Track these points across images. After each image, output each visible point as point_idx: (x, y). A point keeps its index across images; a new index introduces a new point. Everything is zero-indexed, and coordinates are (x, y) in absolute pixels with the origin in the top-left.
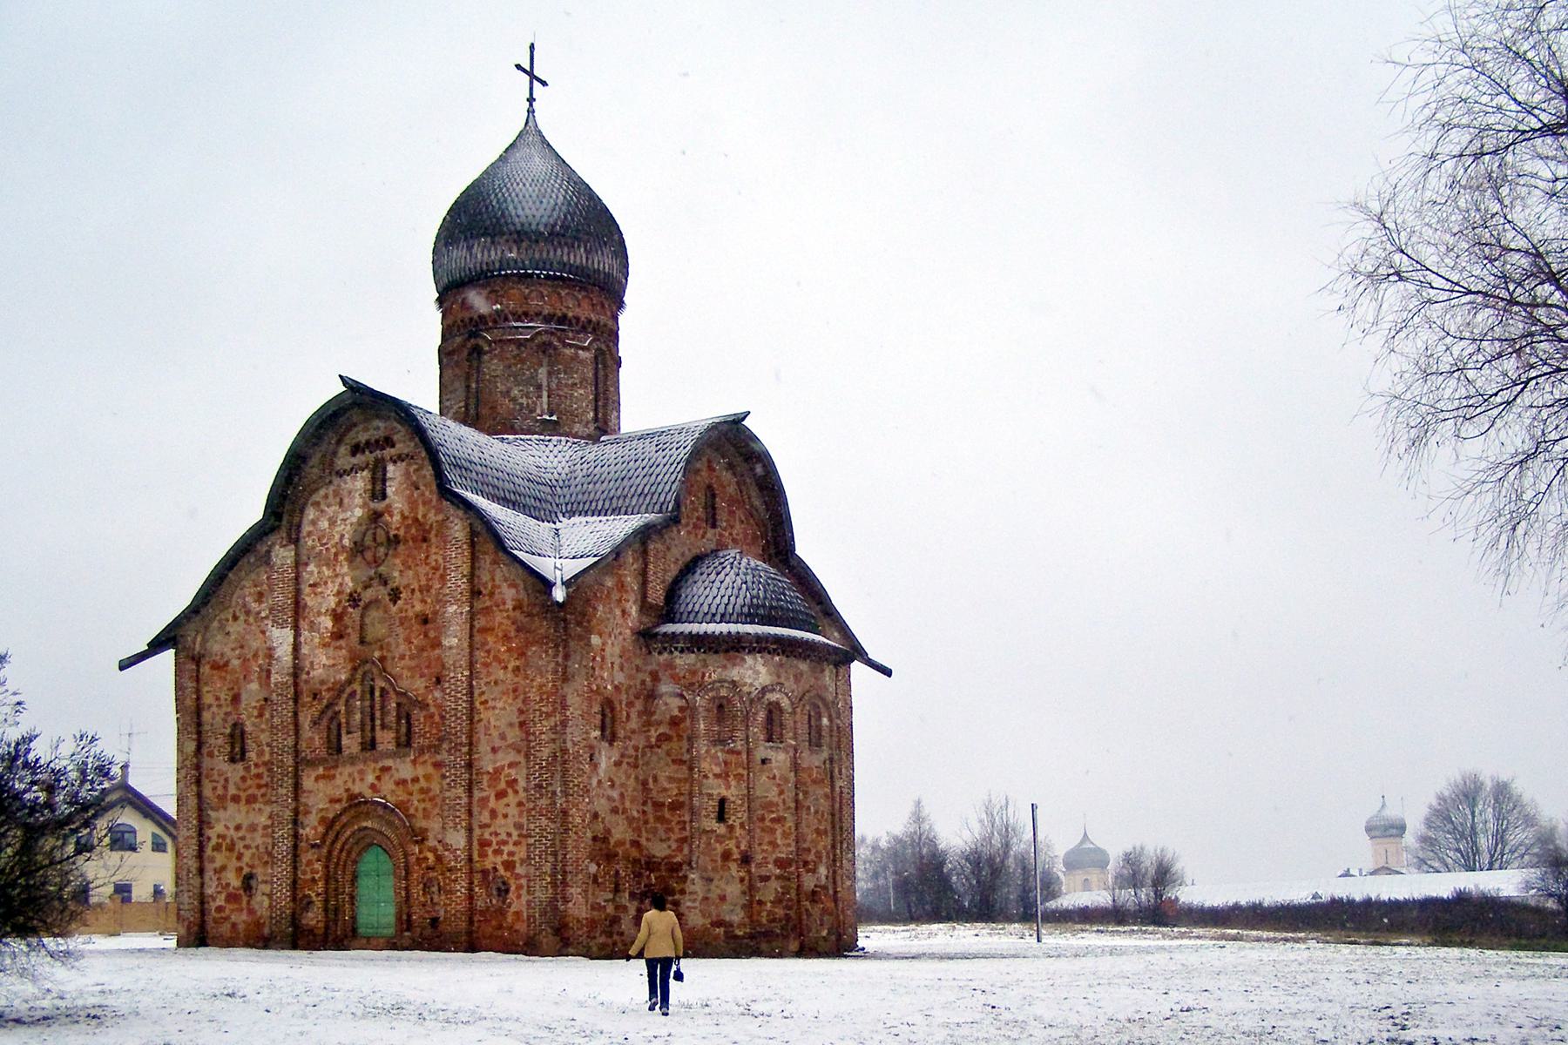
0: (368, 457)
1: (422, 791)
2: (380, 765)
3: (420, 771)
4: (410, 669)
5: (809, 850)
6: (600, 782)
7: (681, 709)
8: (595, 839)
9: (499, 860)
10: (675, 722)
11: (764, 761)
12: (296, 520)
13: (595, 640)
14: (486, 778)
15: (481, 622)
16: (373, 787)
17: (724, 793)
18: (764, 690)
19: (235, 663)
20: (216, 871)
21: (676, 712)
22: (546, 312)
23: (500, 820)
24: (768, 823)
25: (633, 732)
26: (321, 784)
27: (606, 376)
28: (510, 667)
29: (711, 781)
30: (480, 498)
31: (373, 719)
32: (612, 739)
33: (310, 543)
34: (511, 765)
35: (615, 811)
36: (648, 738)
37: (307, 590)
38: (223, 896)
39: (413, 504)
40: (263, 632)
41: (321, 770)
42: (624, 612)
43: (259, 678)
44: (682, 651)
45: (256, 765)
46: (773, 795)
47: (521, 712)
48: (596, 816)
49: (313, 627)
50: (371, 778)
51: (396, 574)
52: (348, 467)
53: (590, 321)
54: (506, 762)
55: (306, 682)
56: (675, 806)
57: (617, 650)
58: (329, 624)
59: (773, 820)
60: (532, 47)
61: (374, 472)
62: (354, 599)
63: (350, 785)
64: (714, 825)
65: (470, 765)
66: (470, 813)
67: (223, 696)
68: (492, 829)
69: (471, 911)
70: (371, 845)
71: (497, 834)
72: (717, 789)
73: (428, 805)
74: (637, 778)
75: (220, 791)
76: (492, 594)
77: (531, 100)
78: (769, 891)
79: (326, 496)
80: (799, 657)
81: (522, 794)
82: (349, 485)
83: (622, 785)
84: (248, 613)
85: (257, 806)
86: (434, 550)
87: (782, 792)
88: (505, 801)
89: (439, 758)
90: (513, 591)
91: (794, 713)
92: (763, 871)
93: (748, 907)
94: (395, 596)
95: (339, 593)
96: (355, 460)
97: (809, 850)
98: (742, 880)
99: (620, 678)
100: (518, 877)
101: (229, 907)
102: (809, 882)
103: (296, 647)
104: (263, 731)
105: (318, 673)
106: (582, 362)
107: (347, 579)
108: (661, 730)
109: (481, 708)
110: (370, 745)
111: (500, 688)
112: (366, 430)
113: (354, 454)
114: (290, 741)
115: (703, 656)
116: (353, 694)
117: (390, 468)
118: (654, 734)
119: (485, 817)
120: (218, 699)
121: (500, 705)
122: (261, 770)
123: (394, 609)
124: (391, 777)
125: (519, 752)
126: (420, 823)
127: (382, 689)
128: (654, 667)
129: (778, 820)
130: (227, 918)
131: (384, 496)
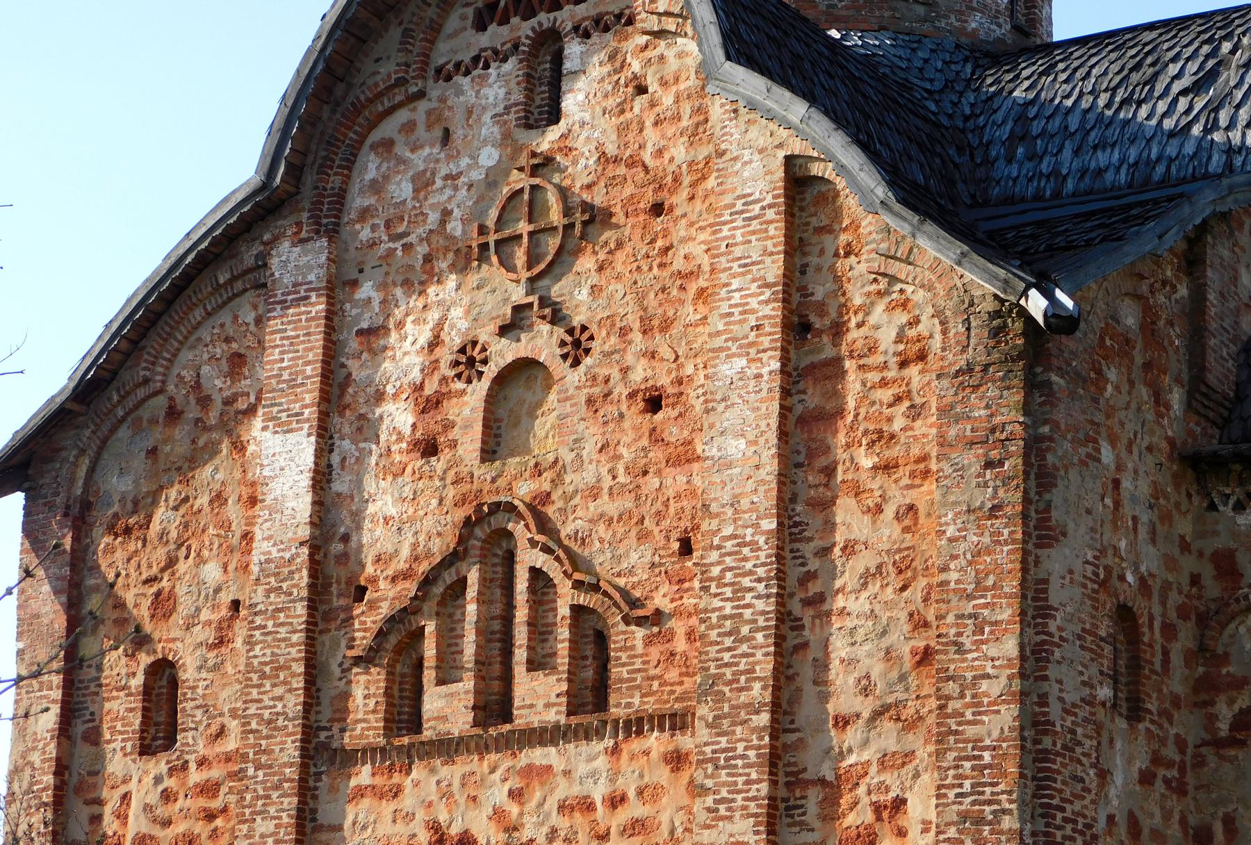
0: (524, 29)
6: (1111, 819)
12: (335, 181)
25: (1176, 702)
28: (889, 511)
31: (507, 653)
32: (1135, 713)
36: (1212, 718)
37: (354, 344)
45: (201, 763)
47: (919, 623)
52: (467, 58)
57: (1144, 488)
61: (531, 59)
62: (469, 360)
74: (1183, 822)
76: (838, 329)
79: (409, 127)
82: (470, 96)
84: (205, 402)
94: (577, 347)
96: (484, 40)
99: (1151, 561)
103: (322, 478)
107: (456, 313)
110: (494, 706)
113: (481, 26)
114: (294, 703)
116: (462, 583)
118: (1225, 713)
122: (216, 773)
123: (573, 377)
128: (1220, 542)
131: (554, 115)
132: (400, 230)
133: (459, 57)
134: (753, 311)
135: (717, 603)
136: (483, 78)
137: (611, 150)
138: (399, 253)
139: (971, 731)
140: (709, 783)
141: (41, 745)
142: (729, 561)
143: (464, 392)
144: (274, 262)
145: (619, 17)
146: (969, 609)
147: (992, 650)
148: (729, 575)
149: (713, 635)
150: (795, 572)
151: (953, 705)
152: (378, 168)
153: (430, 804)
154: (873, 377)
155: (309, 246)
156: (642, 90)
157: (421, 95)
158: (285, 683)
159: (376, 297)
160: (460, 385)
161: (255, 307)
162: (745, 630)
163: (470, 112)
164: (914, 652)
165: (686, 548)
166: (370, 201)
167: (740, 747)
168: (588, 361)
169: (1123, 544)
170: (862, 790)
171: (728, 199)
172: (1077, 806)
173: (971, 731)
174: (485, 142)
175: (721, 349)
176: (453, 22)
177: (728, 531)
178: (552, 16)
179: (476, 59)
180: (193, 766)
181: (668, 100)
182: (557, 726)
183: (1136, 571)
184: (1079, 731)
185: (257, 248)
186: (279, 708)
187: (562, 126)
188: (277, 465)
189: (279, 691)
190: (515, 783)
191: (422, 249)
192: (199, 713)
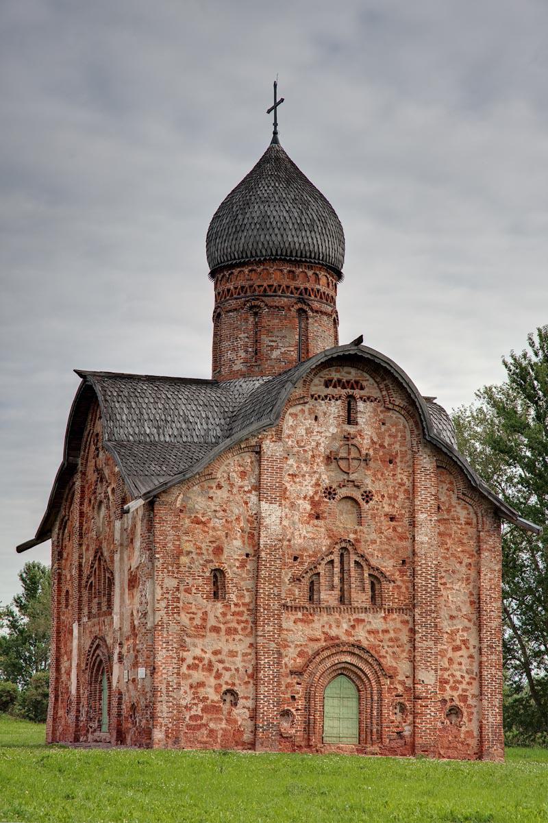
0: (344, 392)
1: (391, 640)
2: (355, 616)
3: (391, 625)
4: (381, 550)
9: (455, 694)
14: (445, 636)
16: (348, 633)
19: (217, 523)
20: (191, 687)
23: (456, 666)
26: (300, 626)
28: (464, 564)
33: (290, 443)
34: (466, 629)
38: (201, 705)
39: (380, 435)
40: (246, 503)
41: (300, 615)
43: (243, 537)
49: (293, 505)
50: (345, 626)
51: (368, 481)
55: (289, 546)
58: (308, 507)
62: (330, 493)
63: (326, 629)
67: (204, 546)
68: (449, 672)
70: (342, 674)
71: (453, 676)
73: (396, 649)
75: (198, 622)
76: (449, 511)
79: (303, 411)
81: (472, 650)
84: (232, 485)
85: (237, 637)
86: (399, 470)
88: (459, 653)
89: (407, 618)
90: (466, 512)
94: (368, 496)
95: (317, 485)
100: (469, 706)
101: (206, 717)
104: (243, 579)
105: (298, 541)
109: (442, 587)
111: (457, 576)
112: (337, 371)
113: (327, 386)
116: (332, 562)
117: (361, 406)
119: (445, 663)
120: (200, 548)
121: (456, 587)
122: (242, 609)
124: (372, 627)
125: (470, 621)
126: (388, 662)
127: (356, 562)
130: (206, 725)
132: (302, 445)
133: (320, 394)
134: (429, 502)
135: (420, 581)
136: (330, 404)
137: (375, 440)
138: (302, 452)
139: (489, 624)
140: (420, 631)
141: (171, 592)
142: (424, 570)
143: (327, 502)
144: (264, 446)
145: (376, 399)
146: (488, 593)
147: (494, 604)
148: (424, 574)
149: (419, 590)
151: (485, 617)
152: (293, 422)
153: (324, 626)
154: (459, 526)
155: (276, 444)
156: (383, 424)
157: (306, 403)
158: (274, 584)
159: (295, 465)
160: (326, 500)
161: (251, 457)
162: (429, 590)
163: (325, 414)
164: (471, 601)
165: (404, 562)
166: (292, 432)
167: (429, 621)
168: (371, 502)
170: (458, 635)
171: (419, 467)
173: (489, 624)
174: (331, 425)
175: (420, 510)
176: (316, 381)
177: (424, 562)
178: (352, 391)
179: (326, 397)
180: (232, 606)
181: (394, 430)
182: (366, 608)
185: (256, 439)
186: (272, 592)
187: (359, 427)
188: (268, 513)
189: (272, 586)
190: (352, 623)
191: (310, 453)
192: (234, 589)
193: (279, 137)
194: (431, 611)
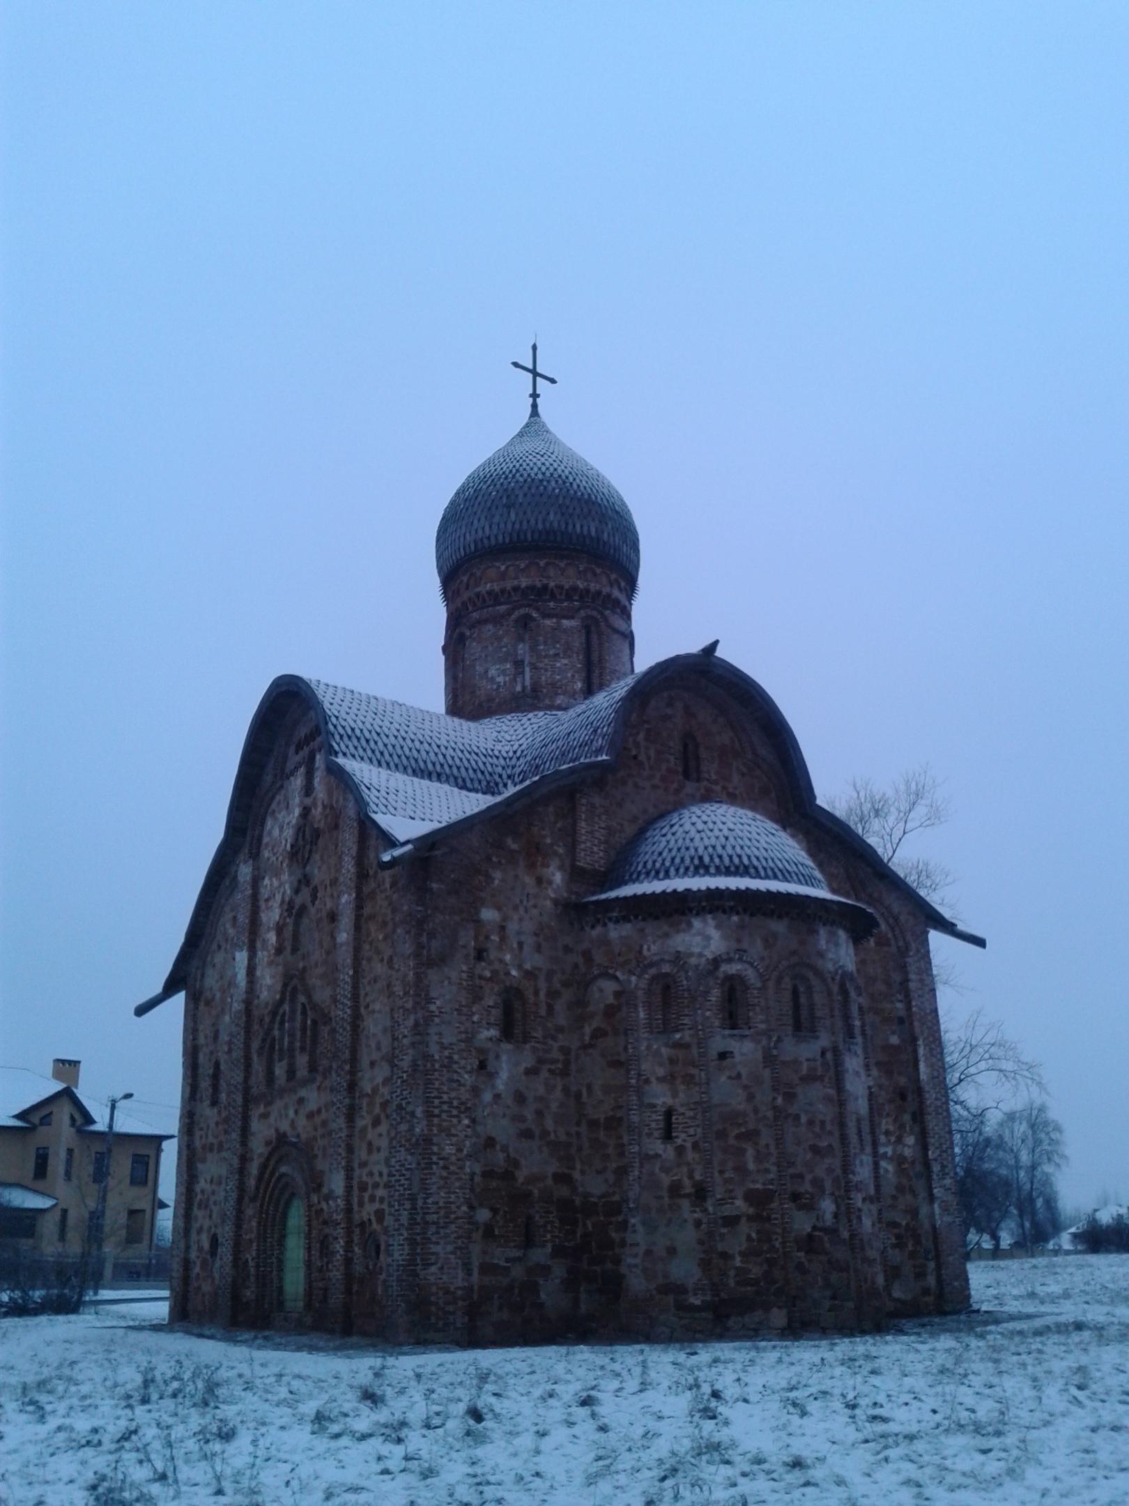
5: (800, 1176)
6: (497, 1097)
7: (618, 994)
8: (487, 1174)
10: (610, 1012)
11: (723, 1056)
13: (488, 914)
15: (367, 910)
17: (669, 1101)
18: (716, 962)
21: (611, 1000)
22: (523, 585)
24: (732, 1141)
25: (560, 1029)
27: (601, 644)
29: (656, 1087)
30: (365, 766)
35: (527, 1134)
42: (539, 881)
44: (617, 921)
46: (738, 1101)
48: (490, 1142)
53: (574, 589)
54: (379, 1080)
56: (613, 1123)
57: (528, 926)
59: (738, 1137)
60: (534, 348)
64: (658, 1147)
65: (352, 1086)
66: (350, 1149)
69: (349, 1276)
71: (371, 1174)
72: (661, 1096)
74: (566, 1090)
77: (535, 395)
78: (736, 1242)
80: (771, 914)
83: (540, 1099)
87: (751, 1097)
91: (764, 988)
92: (727, 1210)
93: (705, 1264)
97: (800, 1176)
98: (698, 1224)
102: (802, 1223)
106: (565, 631)
108: (595, 1024)
115: (642, 924)
118: (588, 1030)
129: (751, 1136)
150: (362, 993)
169: (508, 957)
172: (453, 1094)
183: (520, 967)
184: (456, 1057)
193: (540, 409)
194: (345, 1062)
